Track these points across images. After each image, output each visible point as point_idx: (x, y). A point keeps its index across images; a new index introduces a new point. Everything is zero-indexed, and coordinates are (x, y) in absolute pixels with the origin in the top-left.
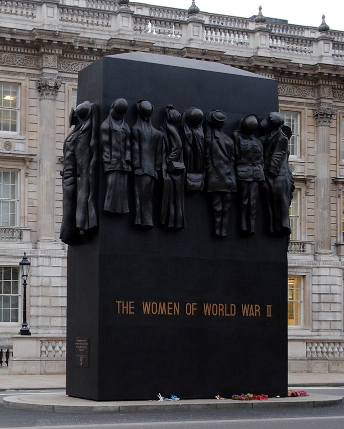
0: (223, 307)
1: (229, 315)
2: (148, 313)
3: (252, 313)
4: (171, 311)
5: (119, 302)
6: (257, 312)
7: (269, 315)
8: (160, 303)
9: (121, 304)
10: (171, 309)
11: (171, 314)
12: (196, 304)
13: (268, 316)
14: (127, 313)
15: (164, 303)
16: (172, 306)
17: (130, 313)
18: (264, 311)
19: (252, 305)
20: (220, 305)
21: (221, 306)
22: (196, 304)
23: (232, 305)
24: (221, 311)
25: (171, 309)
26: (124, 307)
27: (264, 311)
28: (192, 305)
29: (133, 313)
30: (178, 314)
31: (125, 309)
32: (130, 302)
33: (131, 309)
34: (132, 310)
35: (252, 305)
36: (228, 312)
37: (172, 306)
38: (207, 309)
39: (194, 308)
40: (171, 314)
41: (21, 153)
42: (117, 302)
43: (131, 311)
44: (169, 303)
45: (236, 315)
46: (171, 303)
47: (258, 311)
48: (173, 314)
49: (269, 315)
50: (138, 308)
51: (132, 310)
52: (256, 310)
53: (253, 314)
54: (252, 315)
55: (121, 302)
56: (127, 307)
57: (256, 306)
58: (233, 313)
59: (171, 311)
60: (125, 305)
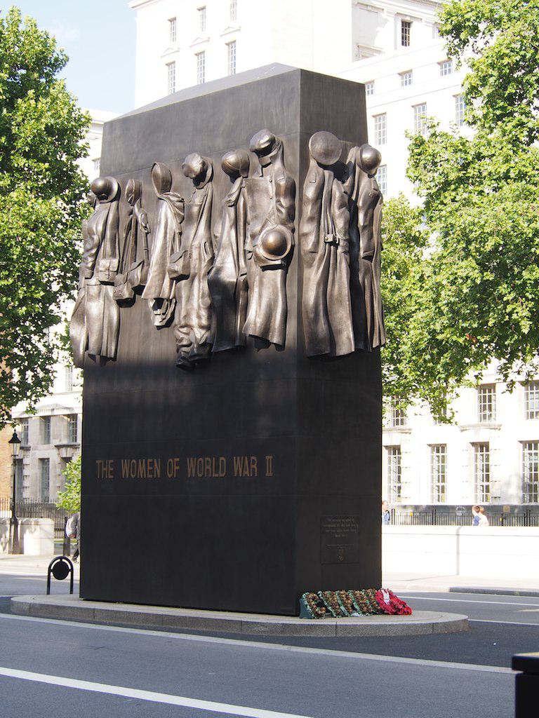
0: (210, 460)
1: (217, 475)
2: (127, 476)
3: (246, 470)
6: (254, 469)
7: (269, 474)
11: (151, 476)
12: (178, 460)
13: (267, 474)
16: (152, 464)
17: (110, 477)
18: (262, 466)
19: (246, 458)
20: (207, 459)
21: (208, 462)
22: (178, 460)
23: (222, 459)
24: (208, 470)
25: (151, 468)
26: (104, 469)
27: (262, 466)
28: (204, 460)
29: (112, 477)
32: (111, 461)
35: (246, 458)
36: (217, 471)
38: (191, 465)
40: (151, 476)
41: (124, 262)
42: (97, 462)
44: (149, 460)
45: (226, 473)
46: (151, 460)
47: (255, 466)
48: (153, 474)
50: (117, 470)
52: (252, 466)
53: (247, 473)
54: (246, 475)
55: (100, 461)
56: (106, 469)
57: (253, 458)
58: (222, 472)
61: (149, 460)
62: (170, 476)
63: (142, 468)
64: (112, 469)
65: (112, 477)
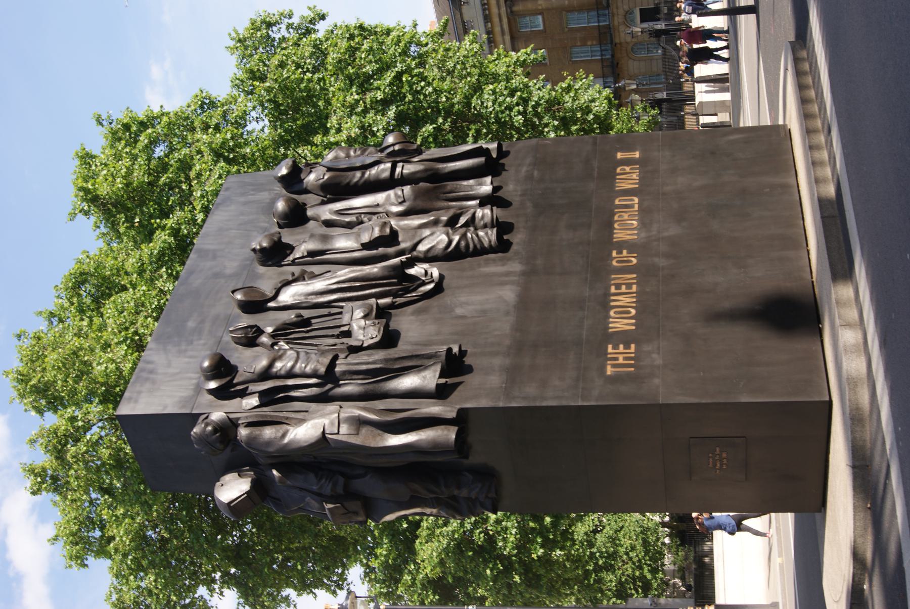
1: (636, 206)
4: (629, 286)
5: (609, 371)
7: (637, 155)
8: (612, 304)
9: (614, 366)
10: (624, 287)
14: (633, 355)
15: (612, 298)
20: (616, 218)
25: (624, 287)
26: (621, 361)
29: (633, 346)
30: (635, 276)
31: (625, 359)
32: (610, 349)
33: (625, 348)
34: (627, 347)
36: (631, 206)
37: (618, 286)
39: (621, 253)
42: (609, 373)
43: (629, 348)
44: (613, 290)
49: (637, 155)
50: (624, 338)
51: (627, 347)
58: (633, 200)
59: (629, 286)
60: (617, 359)
61: (613, 290)
62: (634, 261)
63: (624, 300)
64: (621, 346)
65: (633, 346)
